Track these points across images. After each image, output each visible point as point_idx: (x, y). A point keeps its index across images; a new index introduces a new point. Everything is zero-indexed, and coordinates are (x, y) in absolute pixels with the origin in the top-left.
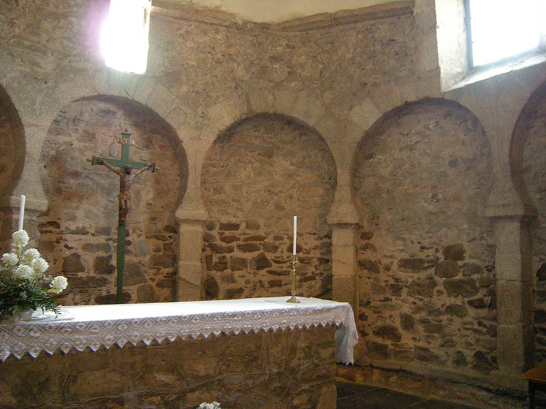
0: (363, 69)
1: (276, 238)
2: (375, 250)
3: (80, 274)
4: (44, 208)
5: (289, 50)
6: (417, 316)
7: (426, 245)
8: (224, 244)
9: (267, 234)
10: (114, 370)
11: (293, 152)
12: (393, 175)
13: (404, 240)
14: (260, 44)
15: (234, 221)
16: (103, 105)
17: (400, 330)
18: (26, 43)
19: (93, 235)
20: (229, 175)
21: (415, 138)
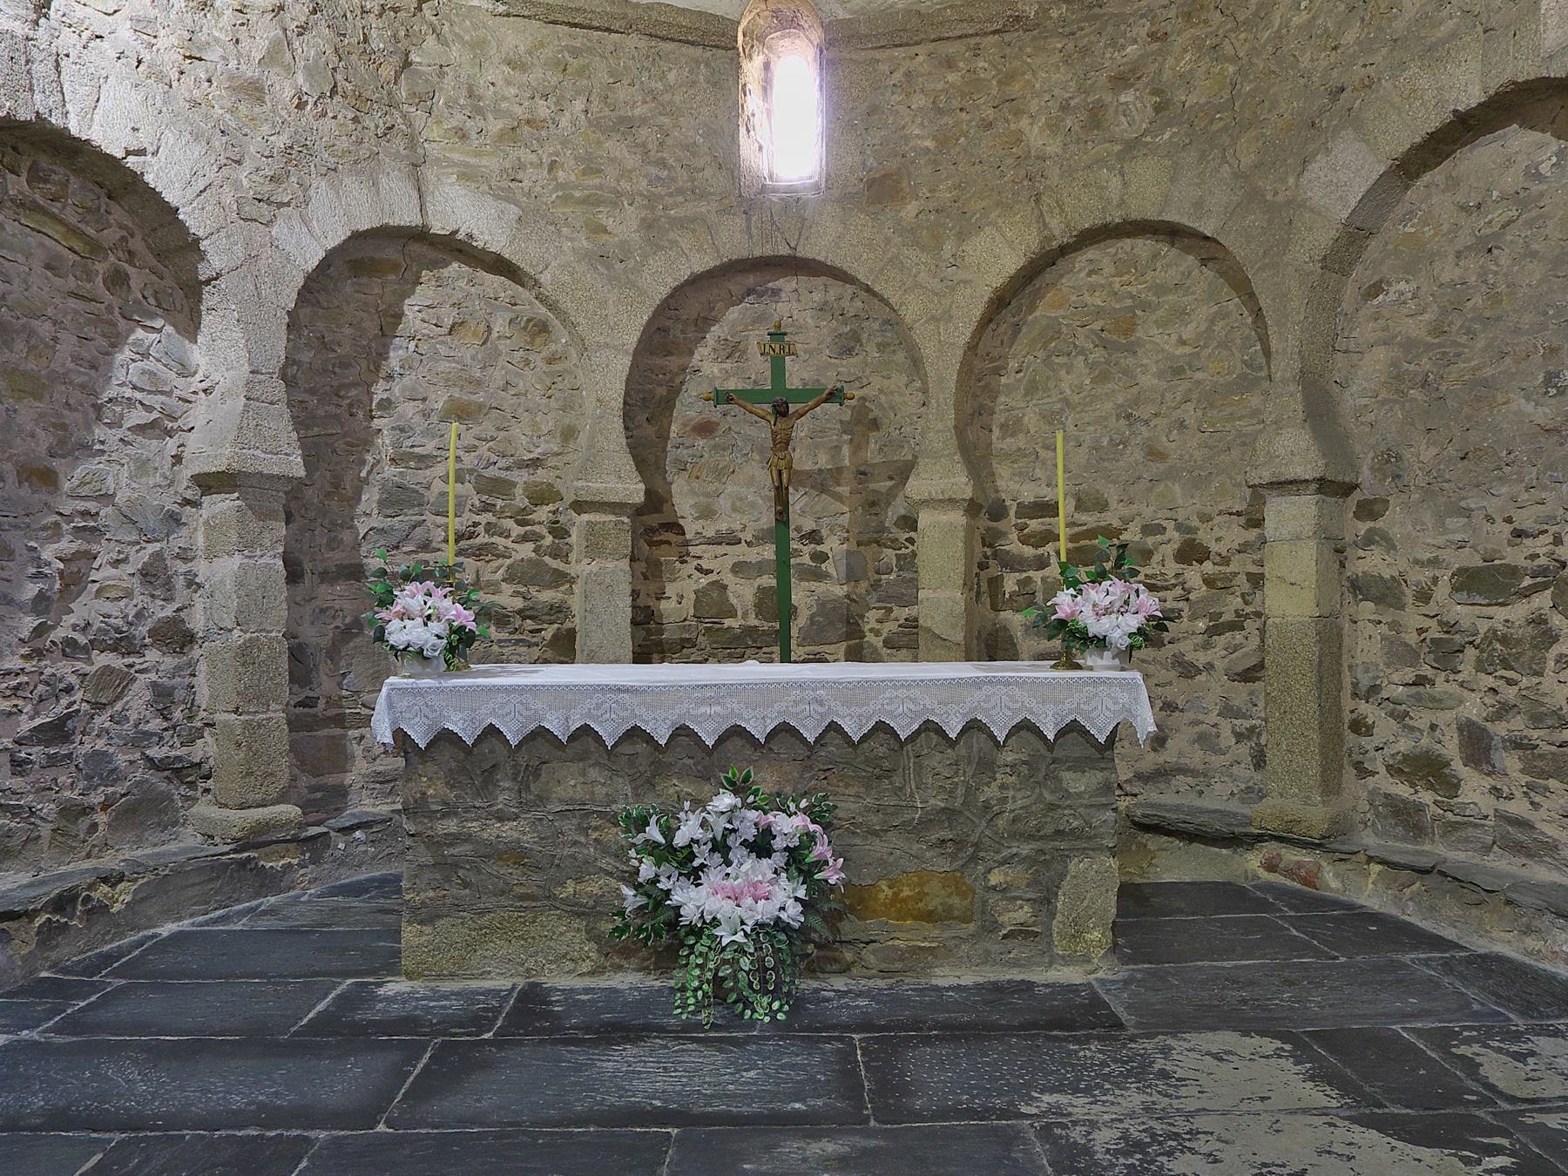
0: (1335, 48)
1: (1148, 530)
2: (1391, 546)
3: (727, 622)
4: (639, 498)
5: (1155, 46)
6: (1500, 729)
7: (1527, 525)
8: (1028, 551)
9: (1126, 521)
10: (596, 764)
11: (1184, 312)
12: (1438, 330)
13: (1467, 513)
14: (1085, 51)
15: (1047, 494)
16: (751, 280)
17: (1458, 766)
18: (577, 194)
19: (749, 544)
20: (1032, 389)
21: (1498, 215)
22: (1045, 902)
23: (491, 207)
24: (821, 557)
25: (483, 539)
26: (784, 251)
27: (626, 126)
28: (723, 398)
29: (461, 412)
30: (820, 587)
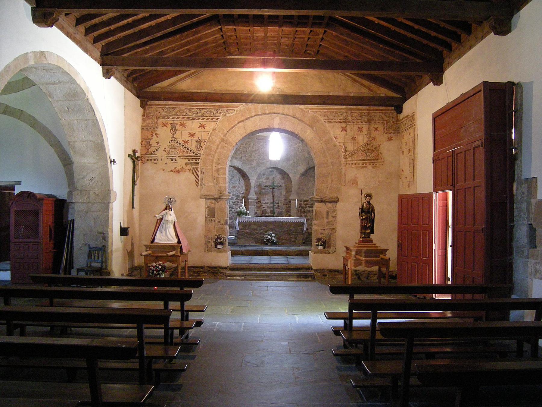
20: (306, 185)
22: (296, 239)
23: (239, 162)
24: (278, 206)
27: (256, 150)
28: (267, 186)
30: (278, 210)
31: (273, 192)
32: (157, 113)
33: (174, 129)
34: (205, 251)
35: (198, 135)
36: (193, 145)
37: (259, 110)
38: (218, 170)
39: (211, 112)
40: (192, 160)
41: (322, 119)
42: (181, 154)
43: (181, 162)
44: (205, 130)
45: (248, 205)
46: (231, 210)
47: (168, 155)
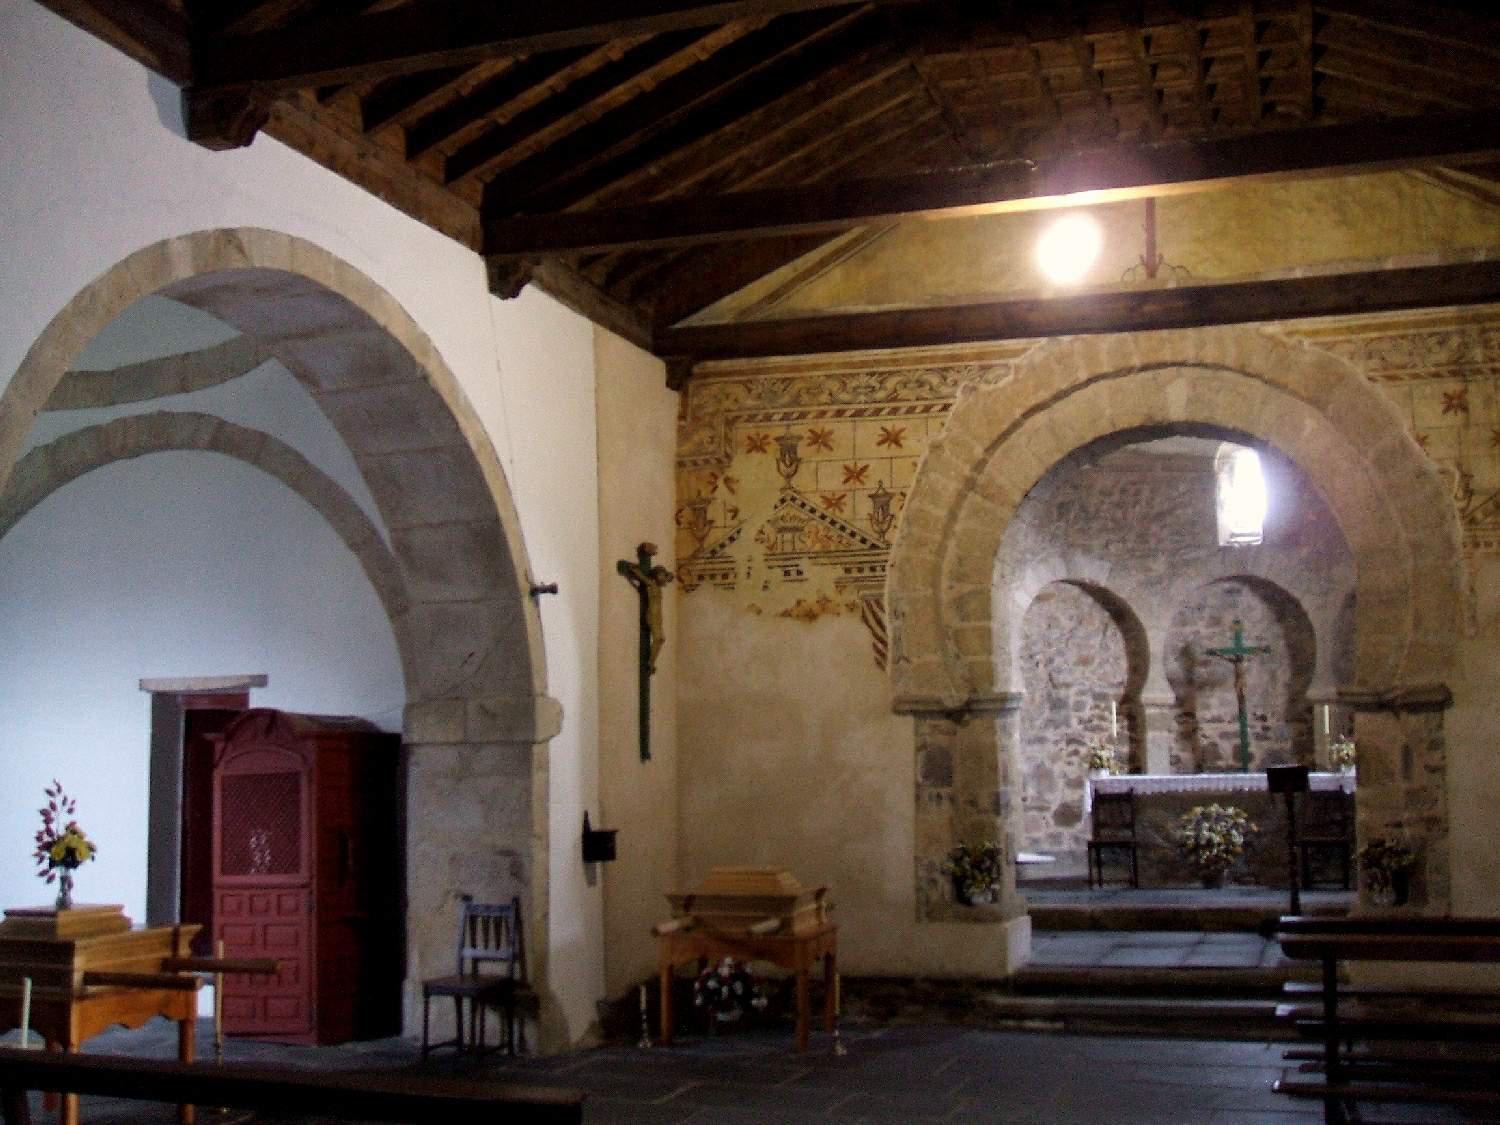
16: (1227, 585)
18: (1138, 554)
19: (1229, 722)
24: (1266, 729)
25: (1095, 722)
26: (1241, 572)
27: (1160, 516)
28: (1211, 652)
29: (1085, 661)
30: (1266, 744)
31: (1238, 675)
32: (728, 404)
33: (789, 456)
34: (918, 919)
35: (877, 474)
36: (859, 510)
37: (1104, 357)
38: (960, 603)
39: (921, 384)
40: (860, 570)
41: (1359, 370)
42: (818, 547)
43: (820, 578)
44: (904, 452)
45: (1143, 731)
46: (1076, 753)
47: (771, 554)
